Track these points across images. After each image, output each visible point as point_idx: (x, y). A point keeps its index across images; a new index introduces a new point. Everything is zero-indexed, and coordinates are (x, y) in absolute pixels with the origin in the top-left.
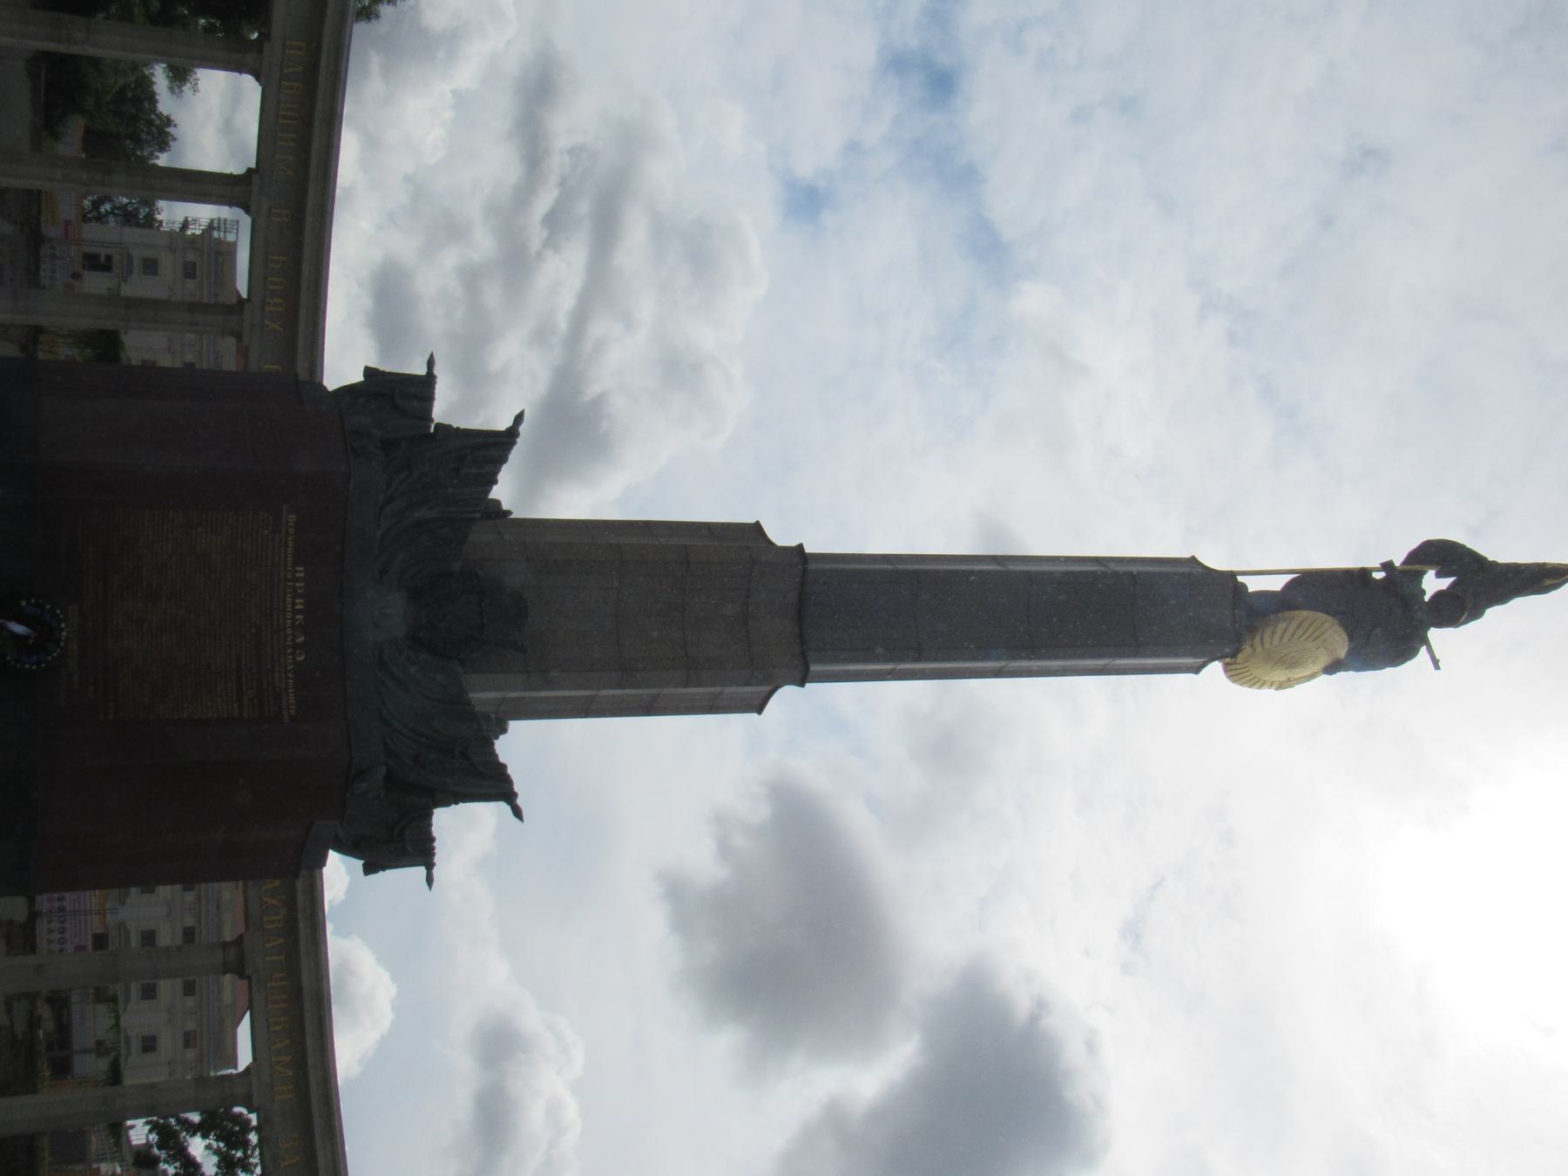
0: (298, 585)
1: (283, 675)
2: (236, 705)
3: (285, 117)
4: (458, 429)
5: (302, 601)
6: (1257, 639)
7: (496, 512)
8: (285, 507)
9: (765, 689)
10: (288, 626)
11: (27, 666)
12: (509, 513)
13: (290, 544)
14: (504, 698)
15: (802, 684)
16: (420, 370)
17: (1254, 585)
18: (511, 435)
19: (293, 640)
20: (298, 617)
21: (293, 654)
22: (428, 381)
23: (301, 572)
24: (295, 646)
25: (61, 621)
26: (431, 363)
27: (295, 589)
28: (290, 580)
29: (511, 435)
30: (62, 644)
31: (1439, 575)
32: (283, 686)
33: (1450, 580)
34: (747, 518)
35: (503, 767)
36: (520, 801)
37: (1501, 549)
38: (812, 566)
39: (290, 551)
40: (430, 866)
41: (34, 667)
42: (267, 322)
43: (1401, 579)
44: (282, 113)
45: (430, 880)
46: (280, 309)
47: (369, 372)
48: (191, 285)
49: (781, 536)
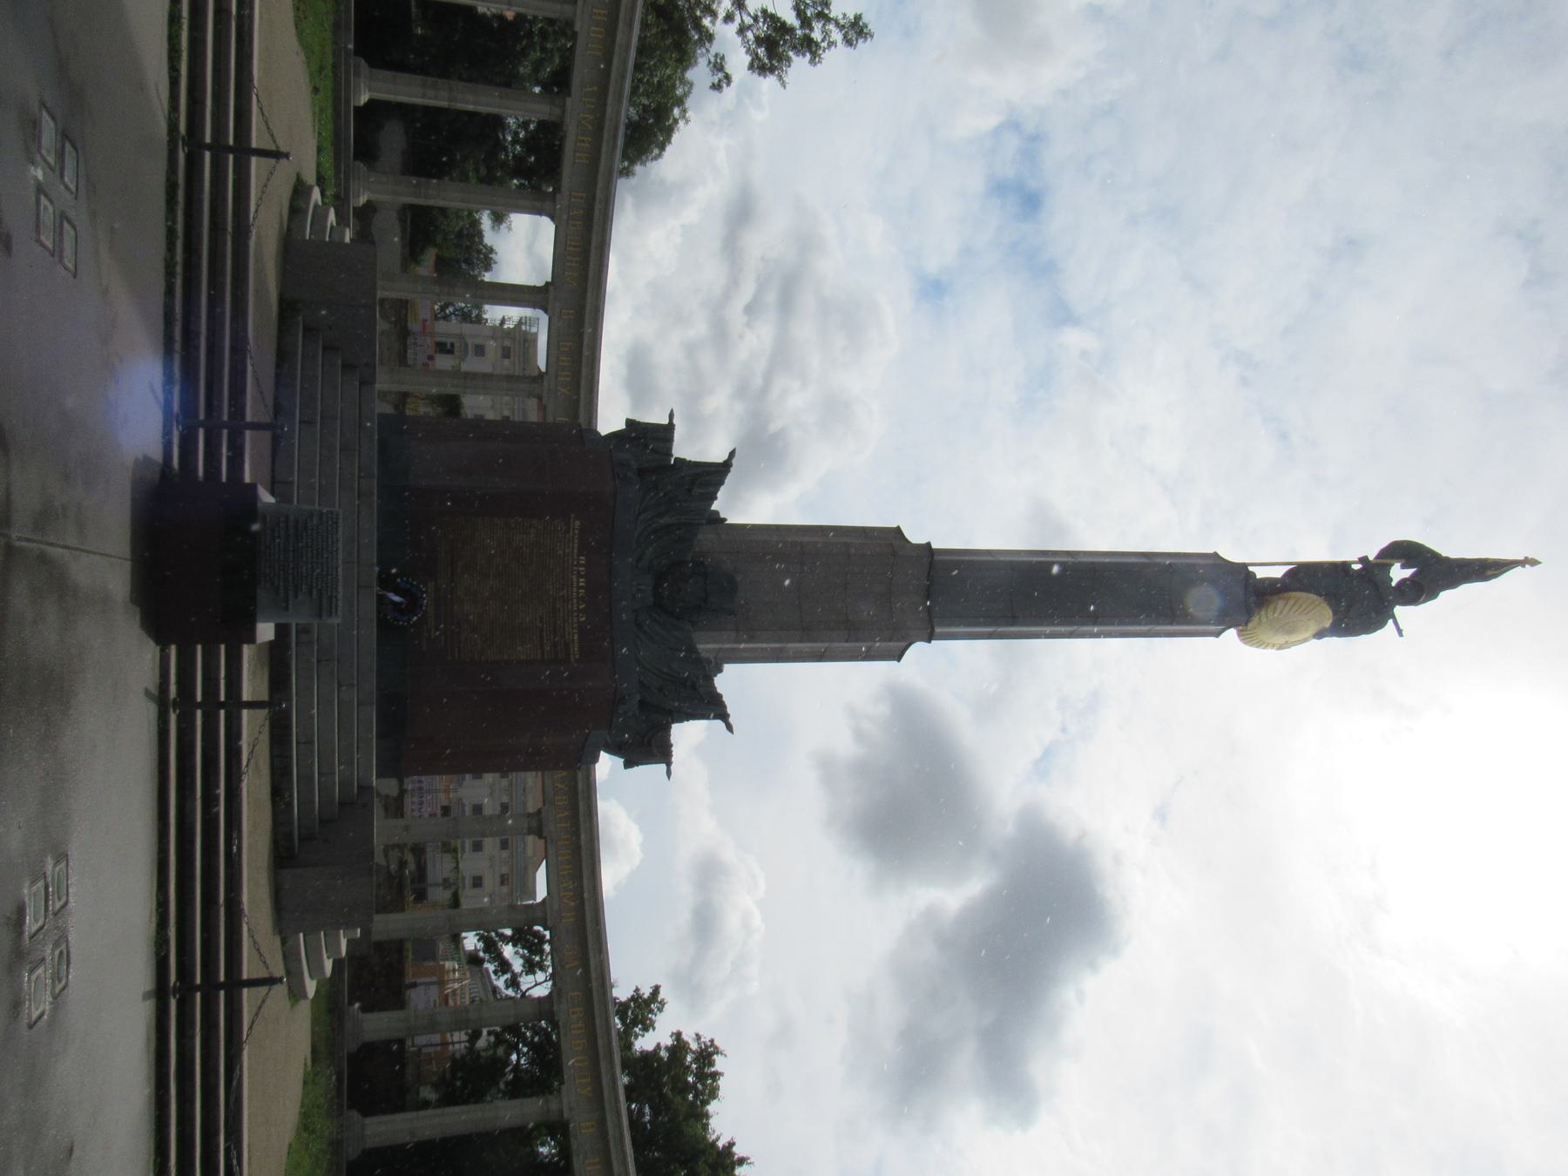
0: (581, 569)
2: (539, 651)
4: (690, 461)
6: (1263, 613)
7: (716, 520)
8: (572, 515)
9: (904, 644)
11: (401, 623)
12: (725, 520)
13: (576, 541)
14: (720, 648)
15: (929, 642)
16: (666, 422)
17: (1261, 573)
18: (725, 467)
19: (578, 607)
20: (581, 591)
21: (578, 616)
24: (579, 611)
25: (423, 592)
26: (671, 416)
27: (579, 572)
29: (725, 467)
30: (424, 608)
31: (1403, 567)
33: (1412, 570)
34: (891, 523)
35: (720, 696)
37: (1451, 547)
38: (936, 557)
39: (576, 545)
40: (669, 764)
41: (406, 624)
42: (559, 388)
43: (1373, 570)
45: (669, 773)
46: (568, 379)
47: (630, 423)
48: (506, 362)
49: (915, 536)
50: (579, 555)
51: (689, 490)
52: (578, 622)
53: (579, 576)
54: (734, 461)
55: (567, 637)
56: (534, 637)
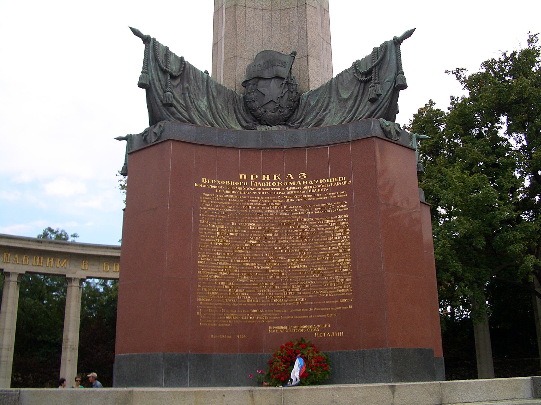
0: (252, 178)
1: (316, 187)
3: (40, 262)
5: (264, 176)
10: (281, 185)
16: (125, 142)
18: (146, 40)
19: (292, 181)
20: (275, 179)
22: (129, 138)
23: (243, 176)
24: (296, 179)
26: (120, 139)
27: (255, 180)
28: (249, 184)
29: (146, 40)
32: (324, 186)
36: (399, 35)
39: (227, 183)
44: (38, 264)
50: (240, 181)
51: (173, 77)
52: (308, 179)
53: (260, 180)
54: (145, 33)
55: (324, 190)
56: (325, 222)
